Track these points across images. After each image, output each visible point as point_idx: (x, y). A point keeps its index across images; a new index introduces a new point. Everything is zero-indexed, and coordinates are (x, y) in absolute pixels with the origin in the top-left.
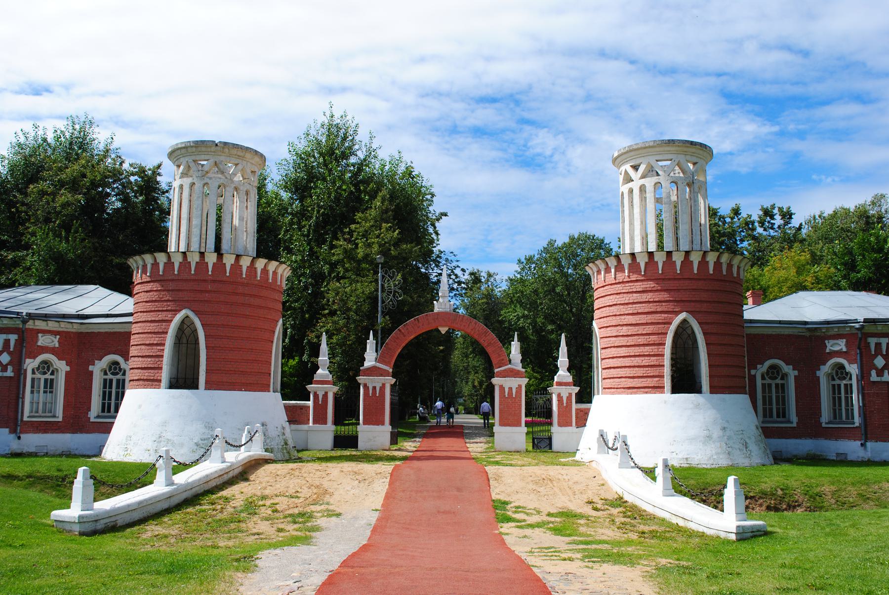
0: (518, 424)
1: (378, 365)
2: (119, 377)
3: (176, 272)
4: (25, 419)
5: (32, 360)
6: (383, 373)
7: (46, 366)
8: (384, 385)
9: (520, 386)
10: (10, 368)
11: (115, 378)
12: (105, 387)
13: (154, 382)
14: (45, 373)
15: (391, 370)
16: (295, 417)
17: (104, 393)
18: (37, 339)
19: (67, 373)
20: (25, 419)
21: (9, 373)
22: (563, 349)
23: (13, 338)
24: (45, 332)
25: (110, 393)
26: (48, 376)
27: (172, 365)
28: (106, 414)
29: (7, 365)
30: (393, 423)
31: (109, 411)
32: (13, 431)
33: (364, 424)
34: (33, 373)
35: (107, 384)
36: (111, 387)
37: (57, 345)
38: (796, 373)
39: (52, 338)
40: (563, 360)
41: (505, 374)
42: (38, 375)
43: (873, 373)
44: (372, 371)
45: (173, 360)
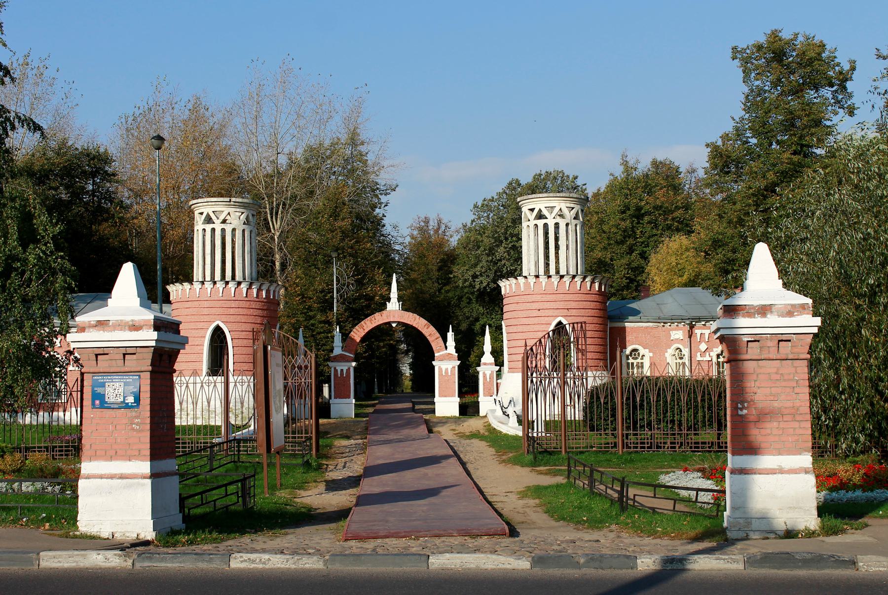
0: (453, 396)
6: (349, 360)
8: (349, 369)
9: (454, 367)
22: (487, 337)
30: (356, 398)
38: (651, 354)
40: (487, 347)
41: (442, 359)
43: (699, 354)
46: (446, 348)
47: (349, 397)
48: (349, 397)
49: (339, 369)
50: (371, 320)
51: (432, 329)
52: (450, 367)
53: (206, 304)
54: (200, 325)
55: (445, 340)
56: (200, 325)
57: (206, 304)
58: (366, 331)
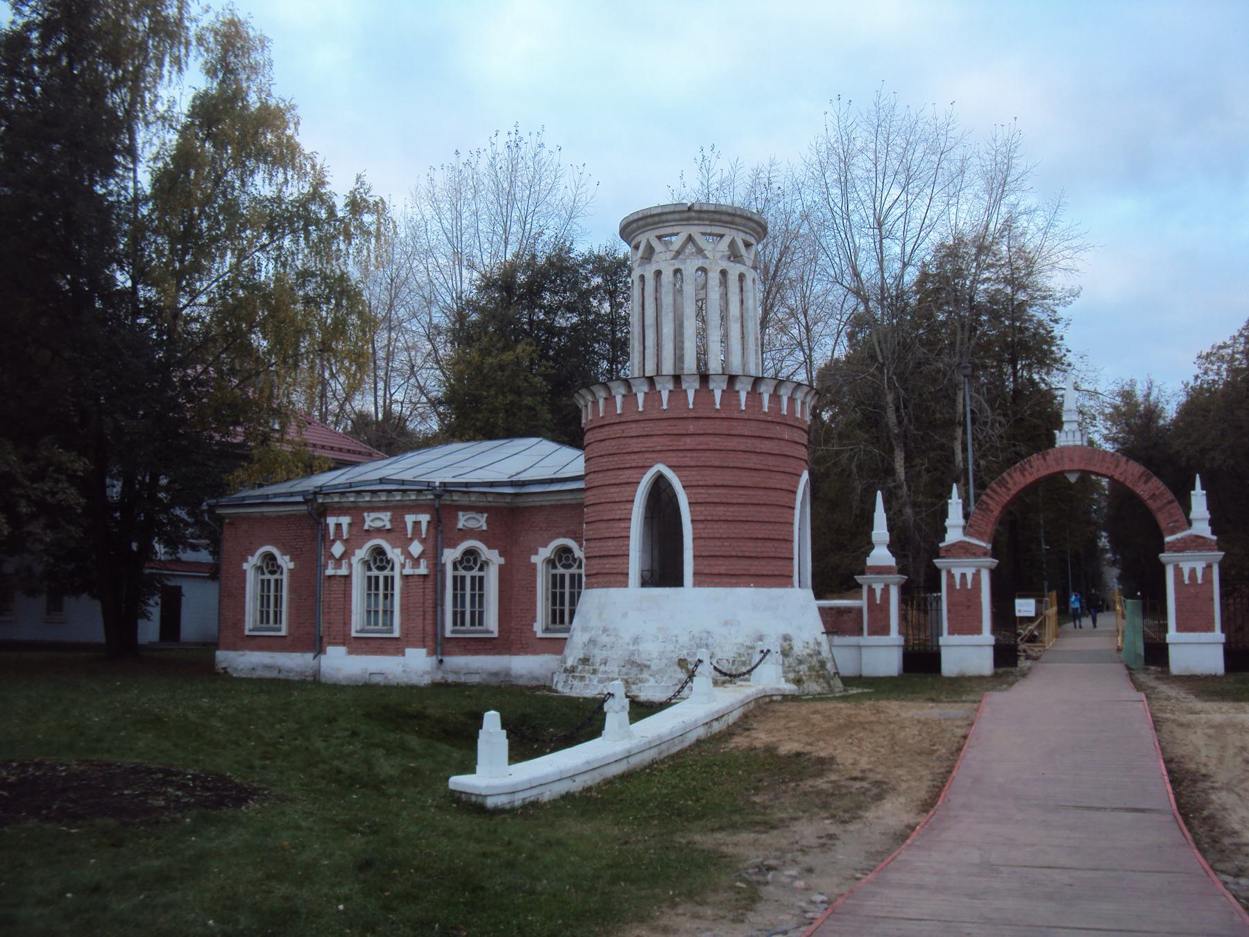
0: (1209, 628)
1: (967, 539)
2: (574, 570)
3: (641, 409)
4: (448, 634)
5: (452, 551)
7: (470, 557)
10: (423, 562)
11: (567, 572)
12: (554, 586)
13: (619, 578)
14: (471, 569)
15: (989, 547)
16: (836, 623)
17: (554, 595)
18: (456, 518)
19: (501, 568)
20: (448, 634)
21: (423, 570)
23: (424, 518)
24: (466, 508)
25: (562, 595)
26: (475, 572)
27: (643, 551)
28: (558, 626)
29: (419, 558)
30: (994, 631)
31: (562, 621)
32: (433, 652)
33: (951, 633)
34: (455, 568)
35: (557, 581)
36: (563, 586)
37: (485, 528)
39: (478, 516)
42: (461, 572)
44: (962, 550)
45: (644, 544)
46: (1189, 523)
47: (978, 630)
48: (978, 630)
49: (957, 573)
50: (1023, 470)
51: (1156, 484)
52: (1200, 567)
53: (635, 429)
54: (624, 476)
55: (1187, 507)
56: (624, 476)
57: (635, 429)
58: (1013, 492)
